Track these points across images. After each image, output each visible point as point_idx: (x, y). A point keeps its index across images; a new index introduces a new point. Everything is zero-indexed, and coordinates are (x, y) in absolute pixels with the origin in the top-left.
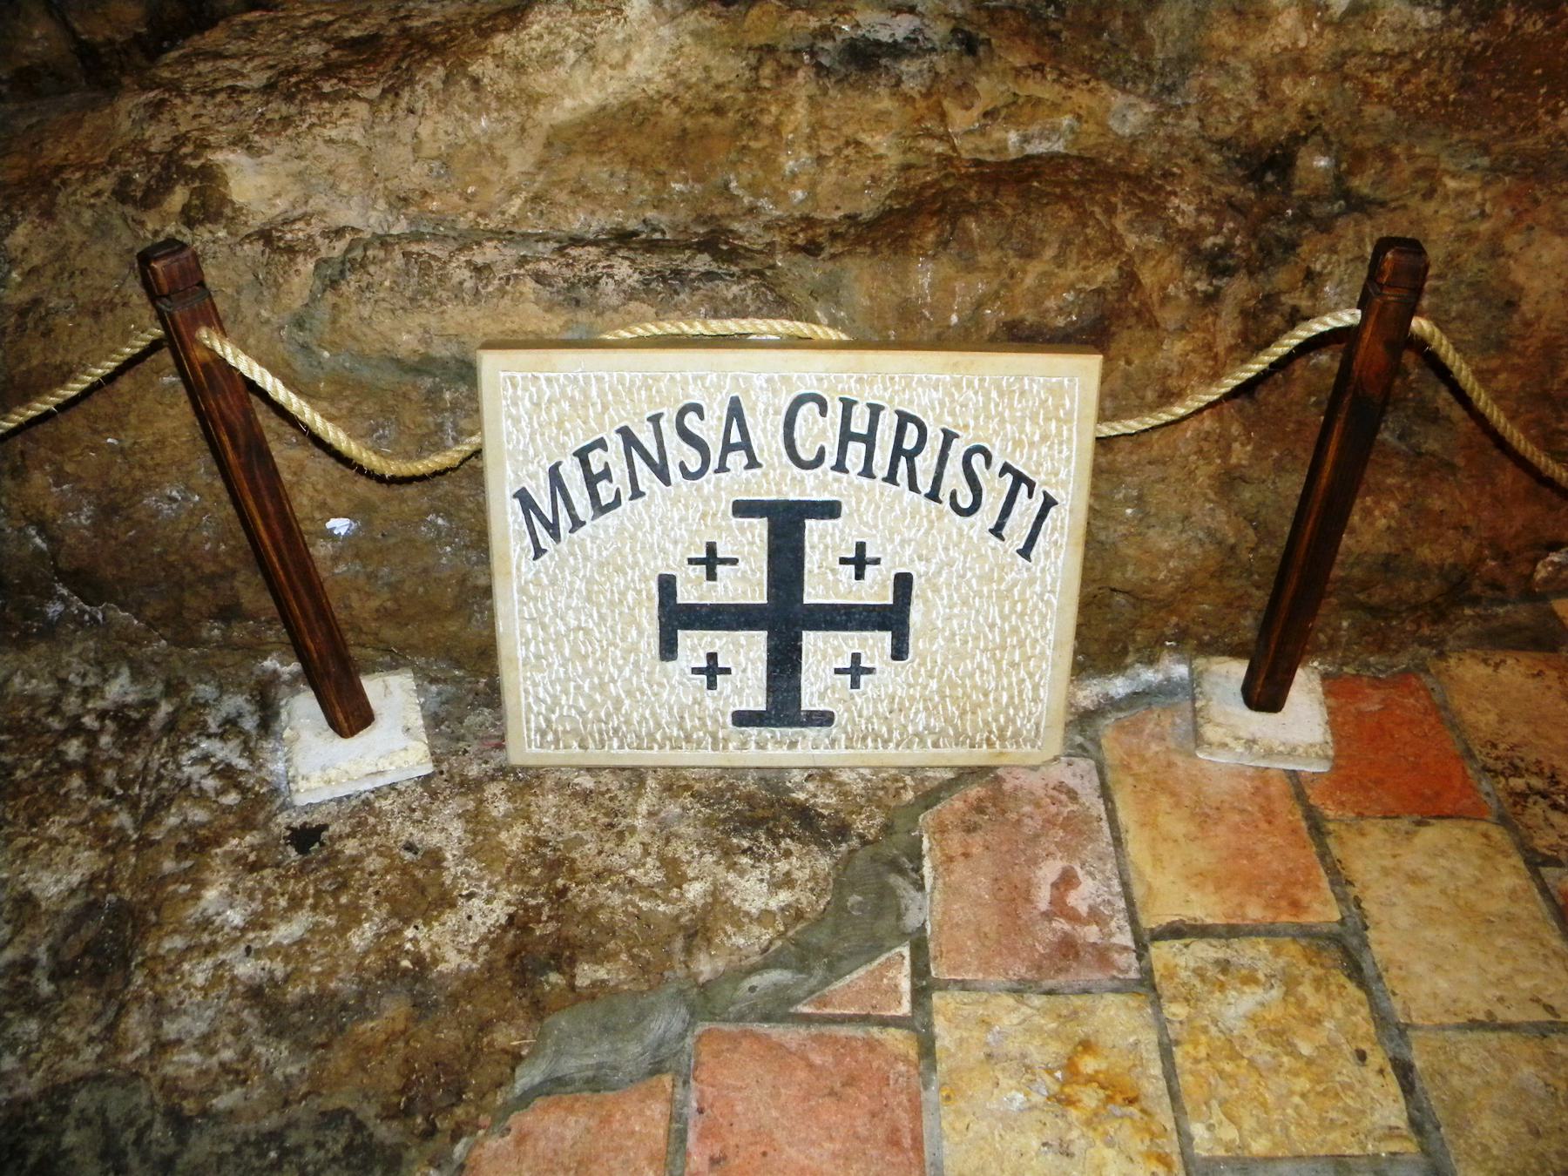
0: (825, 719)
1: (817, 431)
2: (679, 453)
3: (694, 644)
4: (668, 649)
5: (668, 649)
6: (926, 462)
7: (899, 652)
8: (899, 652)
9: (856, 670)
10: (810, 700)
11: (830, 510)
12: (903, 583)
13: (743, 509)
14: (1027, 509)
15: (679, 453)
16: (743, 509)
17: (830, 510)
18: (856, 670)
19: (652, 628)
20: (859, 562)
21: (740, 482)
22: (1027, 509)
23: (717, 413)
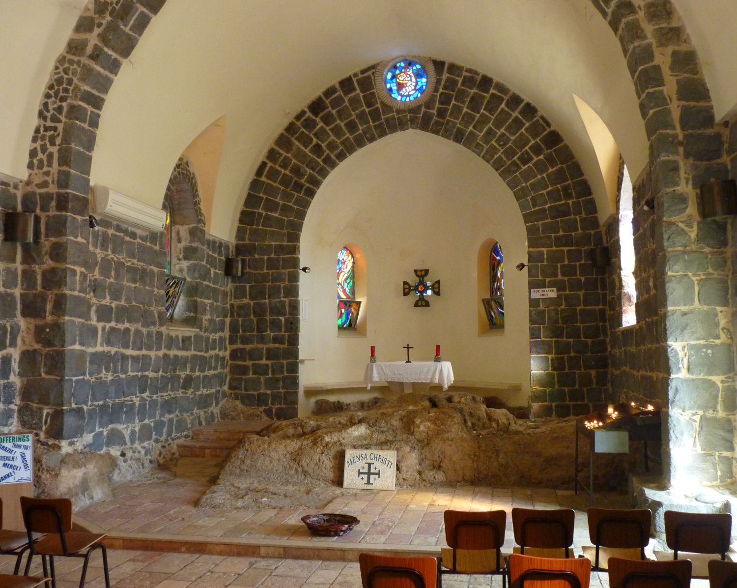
0: (372, 484)
1: (372, 456)
2: (361, 458)
3: (361, 476)
4: (359, 476)
5: (359, 476)
6: (381, 459)
7: (379, 477)
8: (379, 477)
9: (375, 479)
10: (371, 482)
11: (373, 464)
12: (379, 470)
13: (366, 463)
14: (390, 464)
15: (361, 458)
16: (366, 463)
17: (373, 464)
18: (375, 479)
19: (357, 473)
20: (376, 468)
21: (365, 461)
22: (390, 464)
23: (364, 455)
